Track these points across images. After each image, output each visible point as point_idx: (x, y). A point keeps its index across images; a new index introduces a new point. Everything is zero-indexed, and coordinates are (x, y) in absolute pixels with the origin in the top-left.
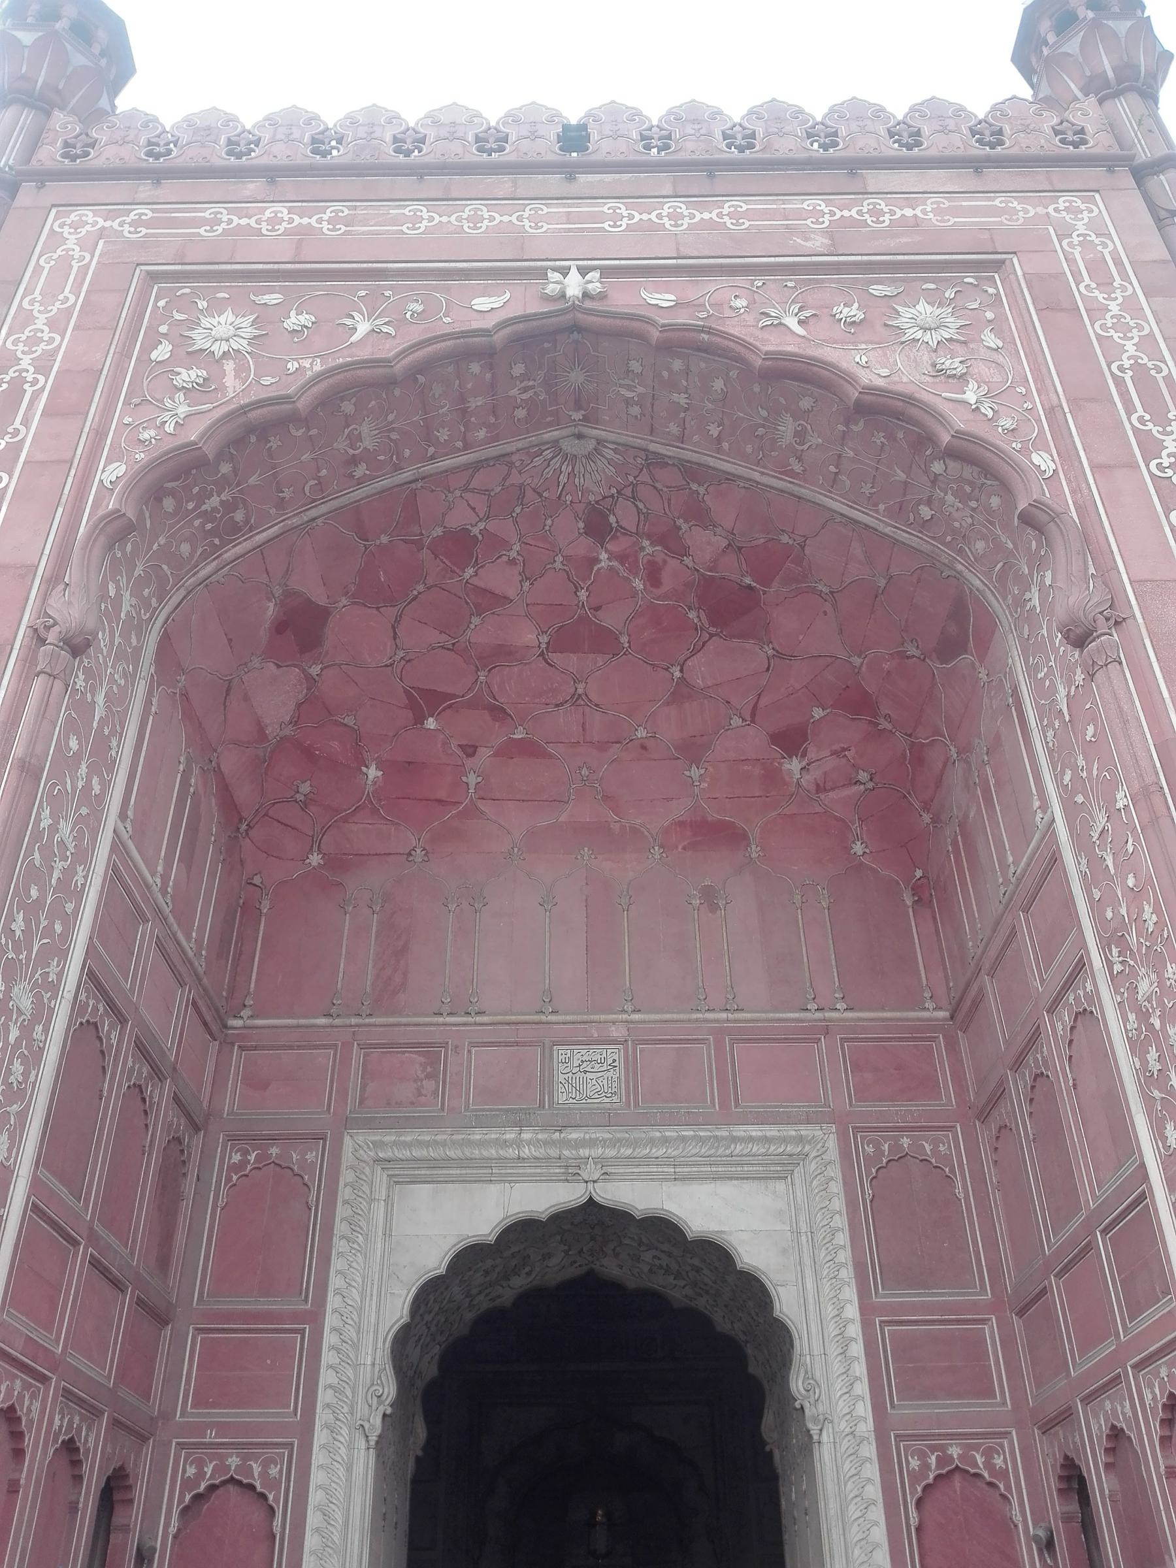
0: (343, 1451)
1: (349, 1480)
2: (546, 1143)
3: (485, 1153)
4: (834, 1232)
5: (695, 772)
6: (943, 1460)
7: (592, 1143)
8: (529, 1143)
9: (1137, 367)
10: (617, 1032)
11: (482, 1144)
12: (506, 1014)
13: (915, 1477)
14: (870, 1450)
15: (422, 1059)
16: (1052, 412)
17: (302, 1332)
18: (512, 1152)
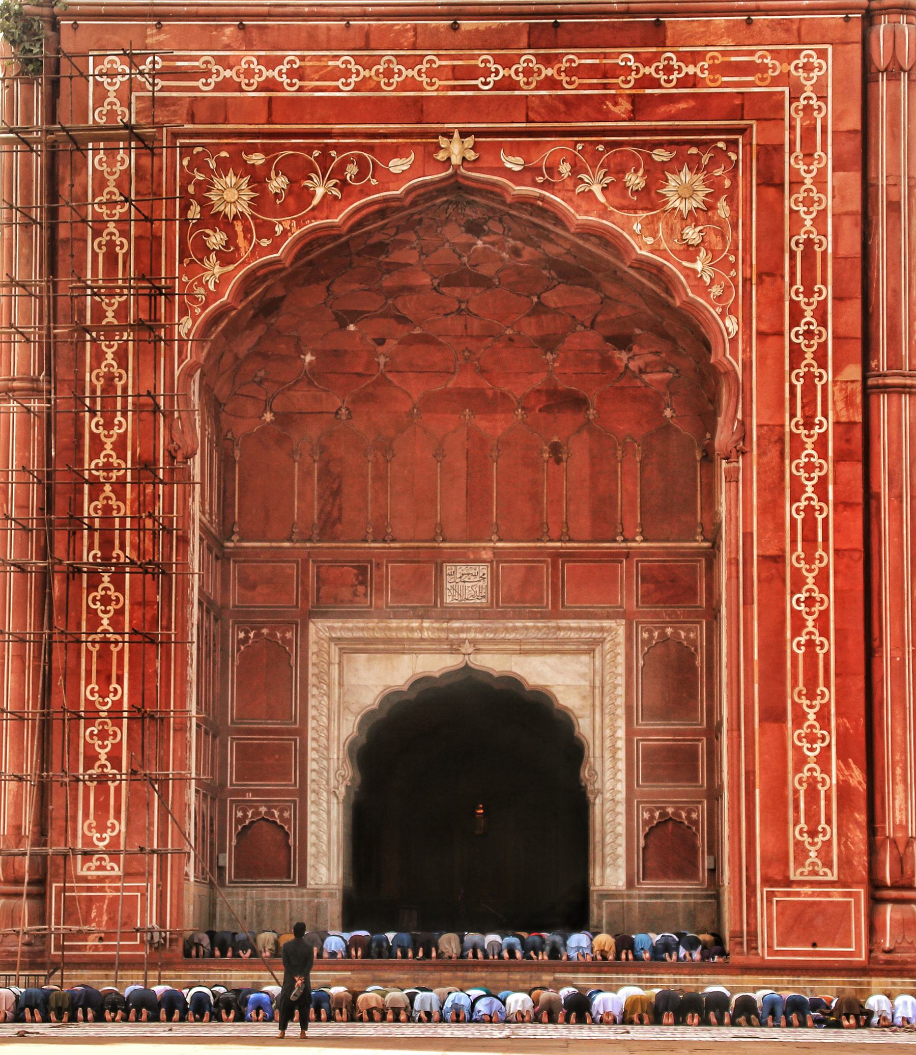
0: (325, 805)
1: (329, 819)
2: (440, 630)
3: (400, 636)
4: (615, 687)
5: (549, 356)
6: (663, 814)
7: (468, 630)
8: (428, 629)
9: (809, 243)
10: (485, 555)
11: (399, 629)
12: (411, 541)
13: (646, 822)
14: (621, 808)
15: (356, 571)
16: (747, 281)
17: (295, 741)
18: (417, 635)
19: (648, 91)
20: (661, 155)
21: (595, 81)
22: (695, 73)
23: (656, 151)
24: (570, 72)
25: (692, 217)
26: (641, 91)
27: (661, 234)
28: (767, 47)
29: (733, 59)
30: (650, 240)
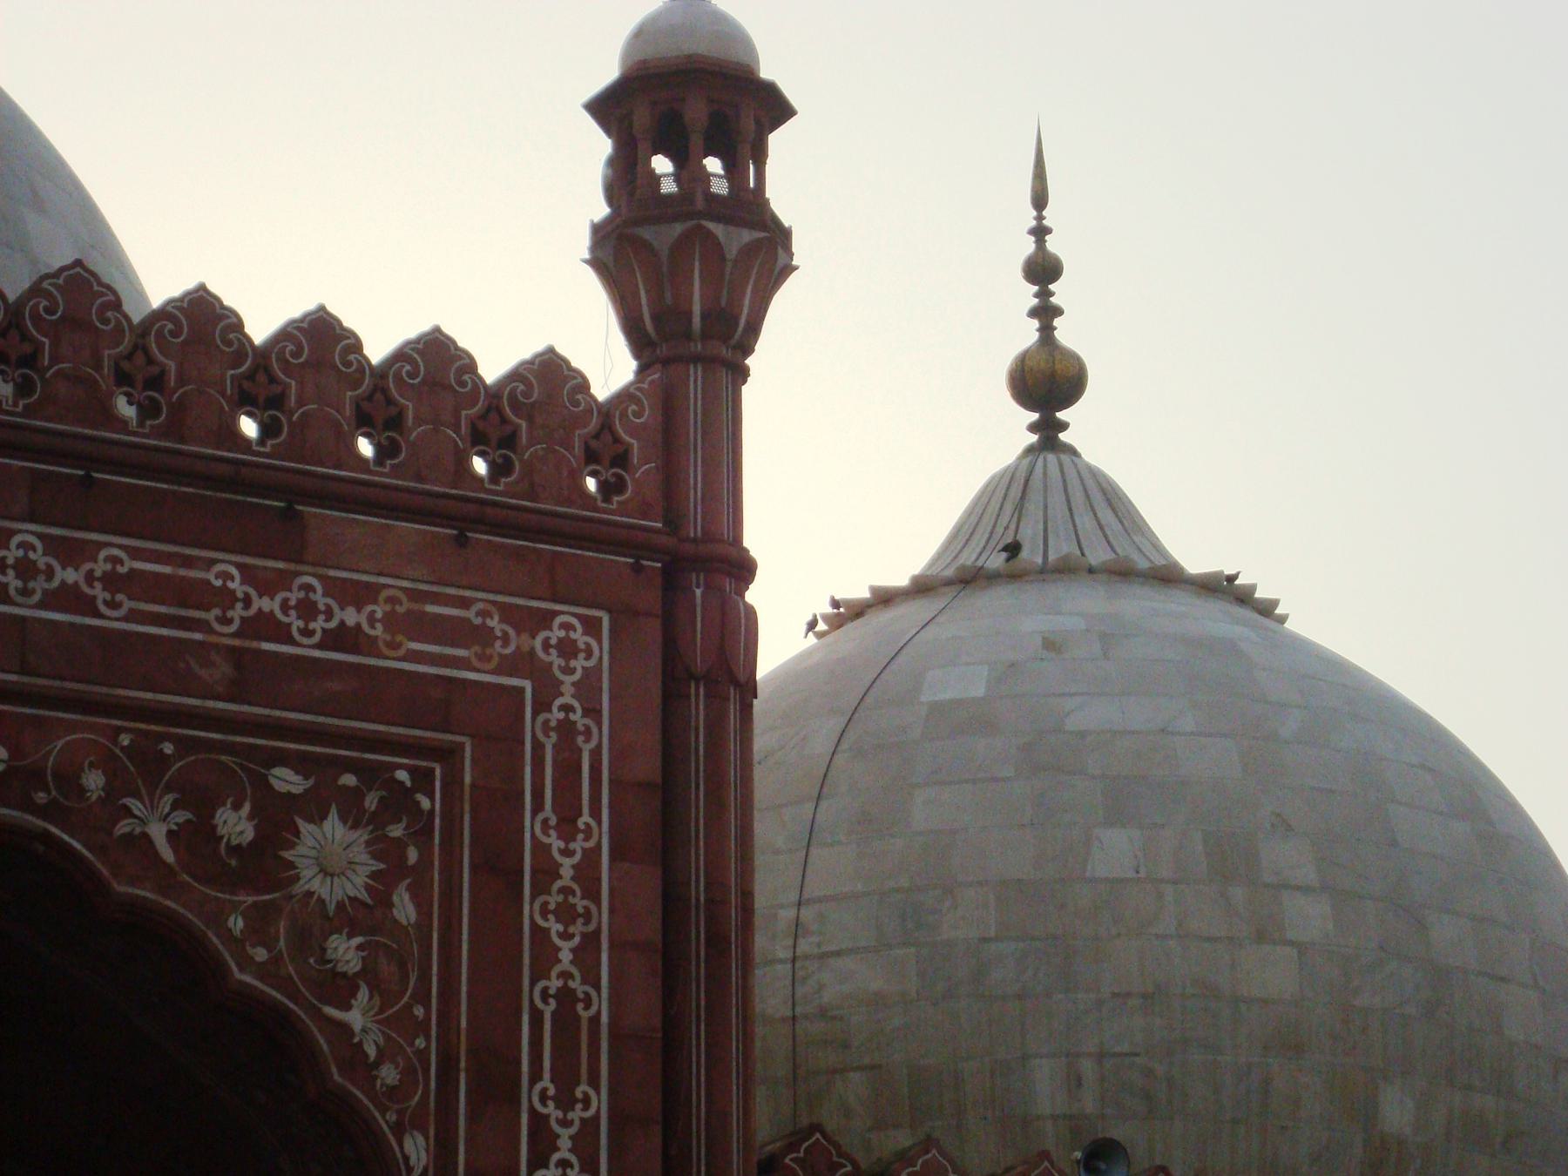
9: (566, 997)
19: (266, 646)
20: (286, 780)
21: (162, 609)
22: (358, 625)
23: (277, 771)
24: (112, 581)
25: (350, 917)
26: (255, 644)
27: (282, 943)
28: (491, 597)
29: (431, 609)
30: (261, 954)
